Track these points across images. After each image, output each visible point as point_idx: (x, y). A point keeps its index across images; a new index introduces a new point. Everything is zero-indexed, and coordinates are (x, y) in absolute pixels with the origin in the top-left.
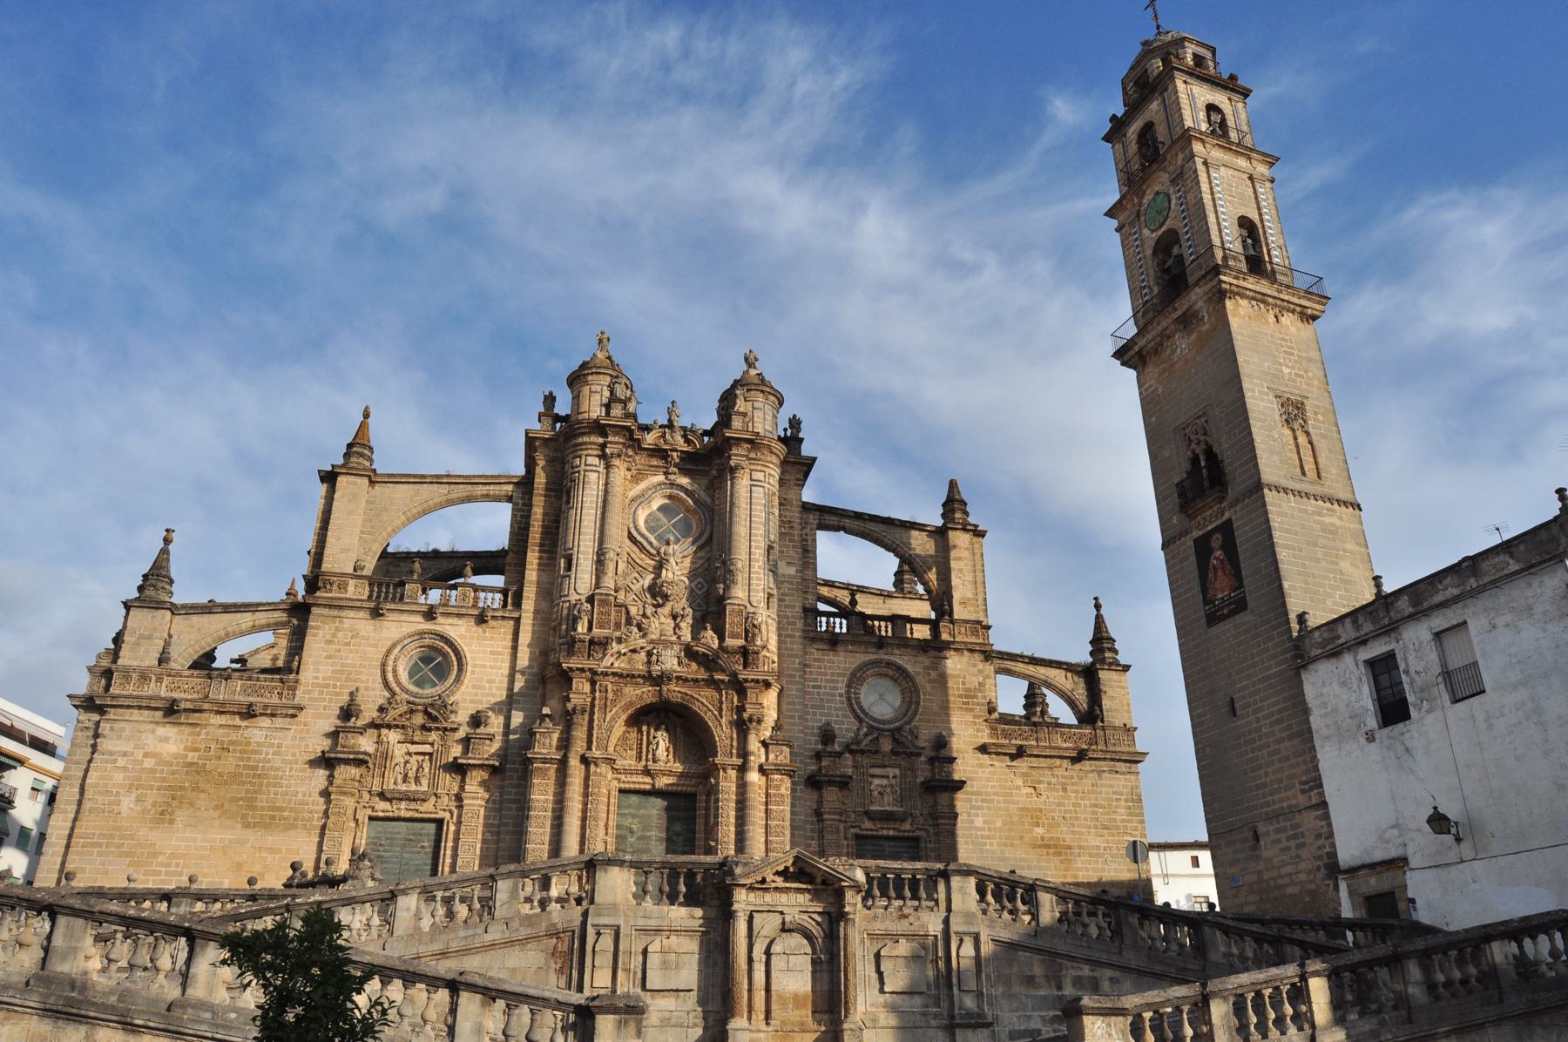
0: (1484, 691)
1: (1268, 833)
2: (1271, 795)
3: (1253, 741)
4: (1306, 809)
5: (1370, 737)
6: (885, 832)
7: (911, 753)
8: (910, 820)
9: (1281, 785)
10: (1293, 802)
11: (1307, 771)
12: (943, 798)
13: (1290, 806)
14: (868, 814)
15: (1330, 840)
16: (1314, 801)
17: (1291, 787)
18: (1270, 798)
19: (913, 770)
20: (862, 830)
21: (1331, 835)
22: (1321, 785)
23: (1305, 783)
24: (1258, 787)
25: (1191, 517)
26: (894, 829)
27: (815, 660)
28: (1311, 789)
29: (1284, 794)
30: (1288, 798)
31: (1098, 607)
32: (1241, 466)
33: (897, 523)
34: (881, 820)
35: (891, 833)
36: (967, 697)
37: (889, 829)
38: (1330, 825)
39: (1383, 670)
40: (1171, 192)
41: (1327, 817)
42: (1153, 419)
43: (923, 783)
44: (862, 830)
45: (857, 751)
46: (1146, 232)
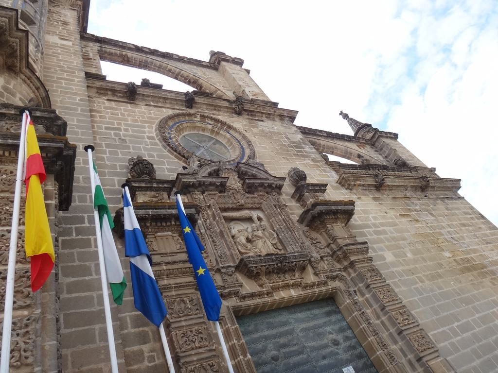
6: (283, 294)
7: (270, 186)
8: (309, 268)
12: (338, 229)
14: (243, 267)
19: (282, 207)
20: (244, 298)
26: (295, 286)
27: (106, 108)
31: (345, 116)
33: (174, 57)
34: (269, 273)
35: (294, 293)
36: (297, 147)
37: (287, 287)
43: (301, 220)
44: (244, 298)
45: (193, 186)
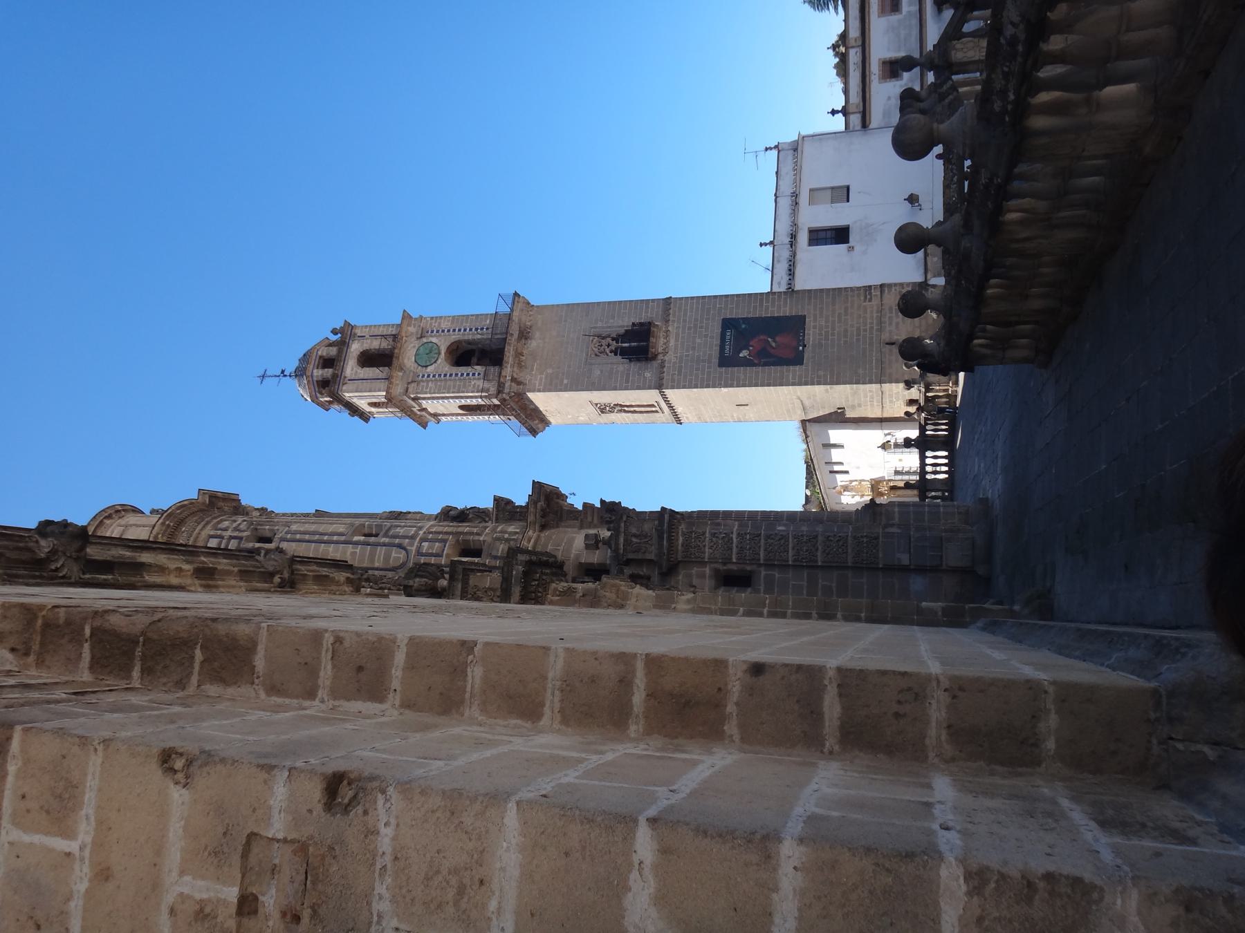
0: (848, 188)
1: (890, 332)
2: (866, 325)
3: (827, 332)
4: (881, 301)
5: (851, 249)
9: (862, 316)
10: (875, 308)
11: (859, 295)
13: (877, 312)
15: (905, 286)
16: (879, 293)
17: (865, 308)
18: (868, 326)
21: (901, 285)
22: (870, 287)
23: (866, 297)
24: (858, 335)
25: (654, 357)
28: (870, 294)
29: (868, 315)
30: (872, 312)
32: (647, 312)
38: (895, 285)
39: (820, 237)
40: (425, 340)
41: (890, 286)
42: (565, 381)
46: (430, 369)
